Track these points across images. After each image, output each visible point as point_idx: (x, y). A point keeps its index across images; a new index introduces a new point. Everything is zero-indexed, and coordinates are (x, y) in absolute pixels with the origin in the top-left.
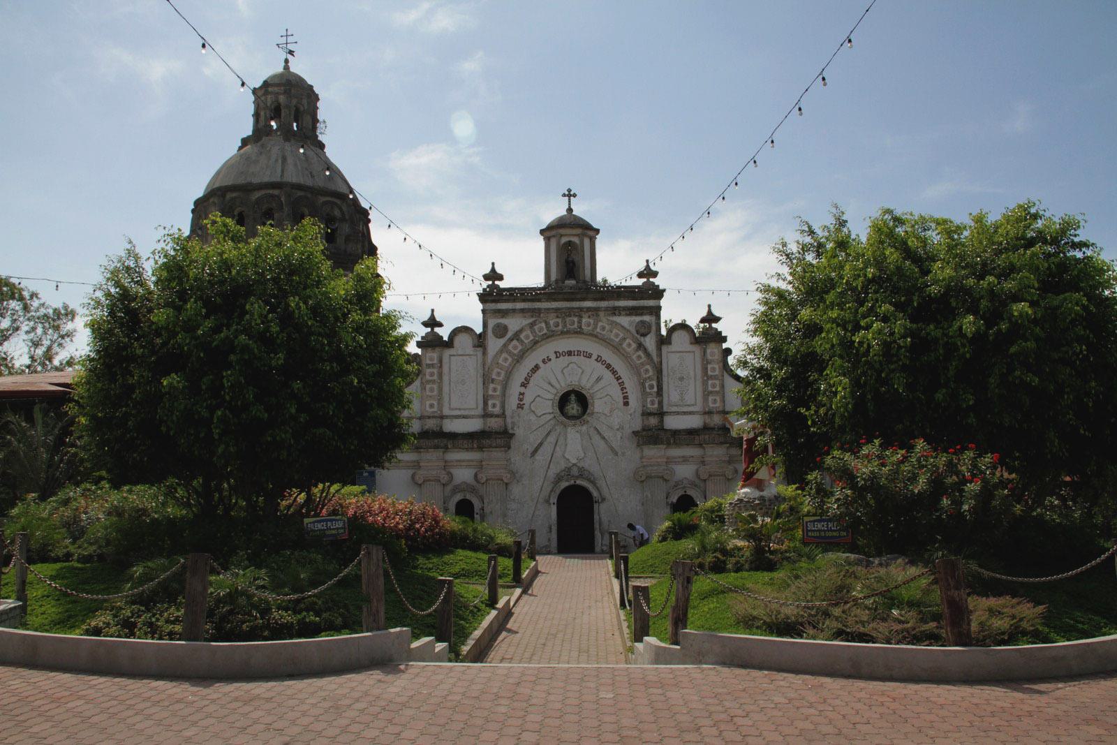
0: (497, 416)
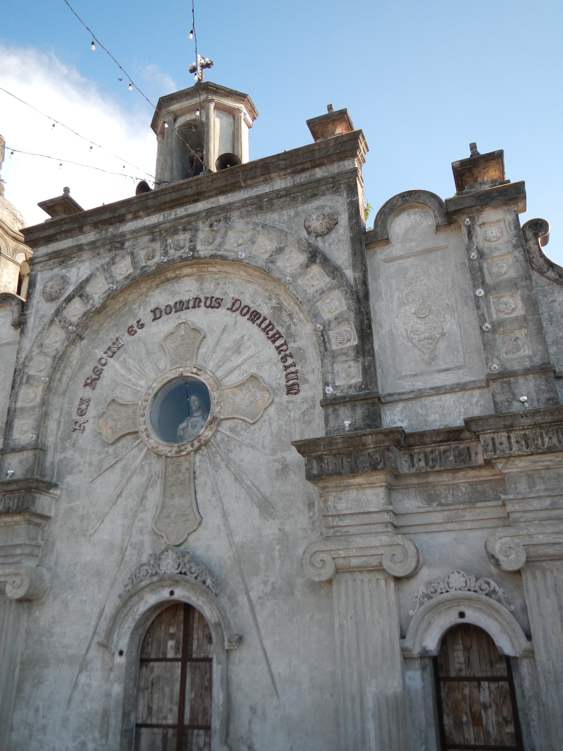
0: (22, 449)
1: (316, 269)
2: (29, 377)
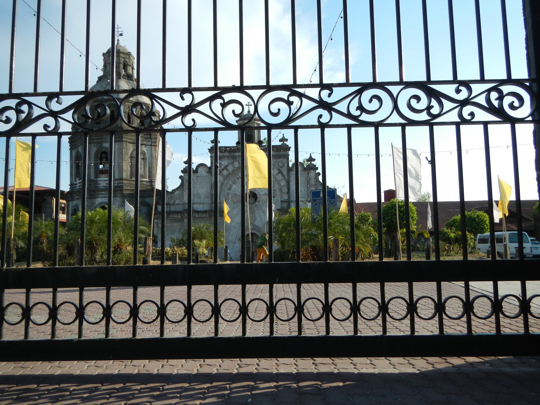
1: (280, 175)
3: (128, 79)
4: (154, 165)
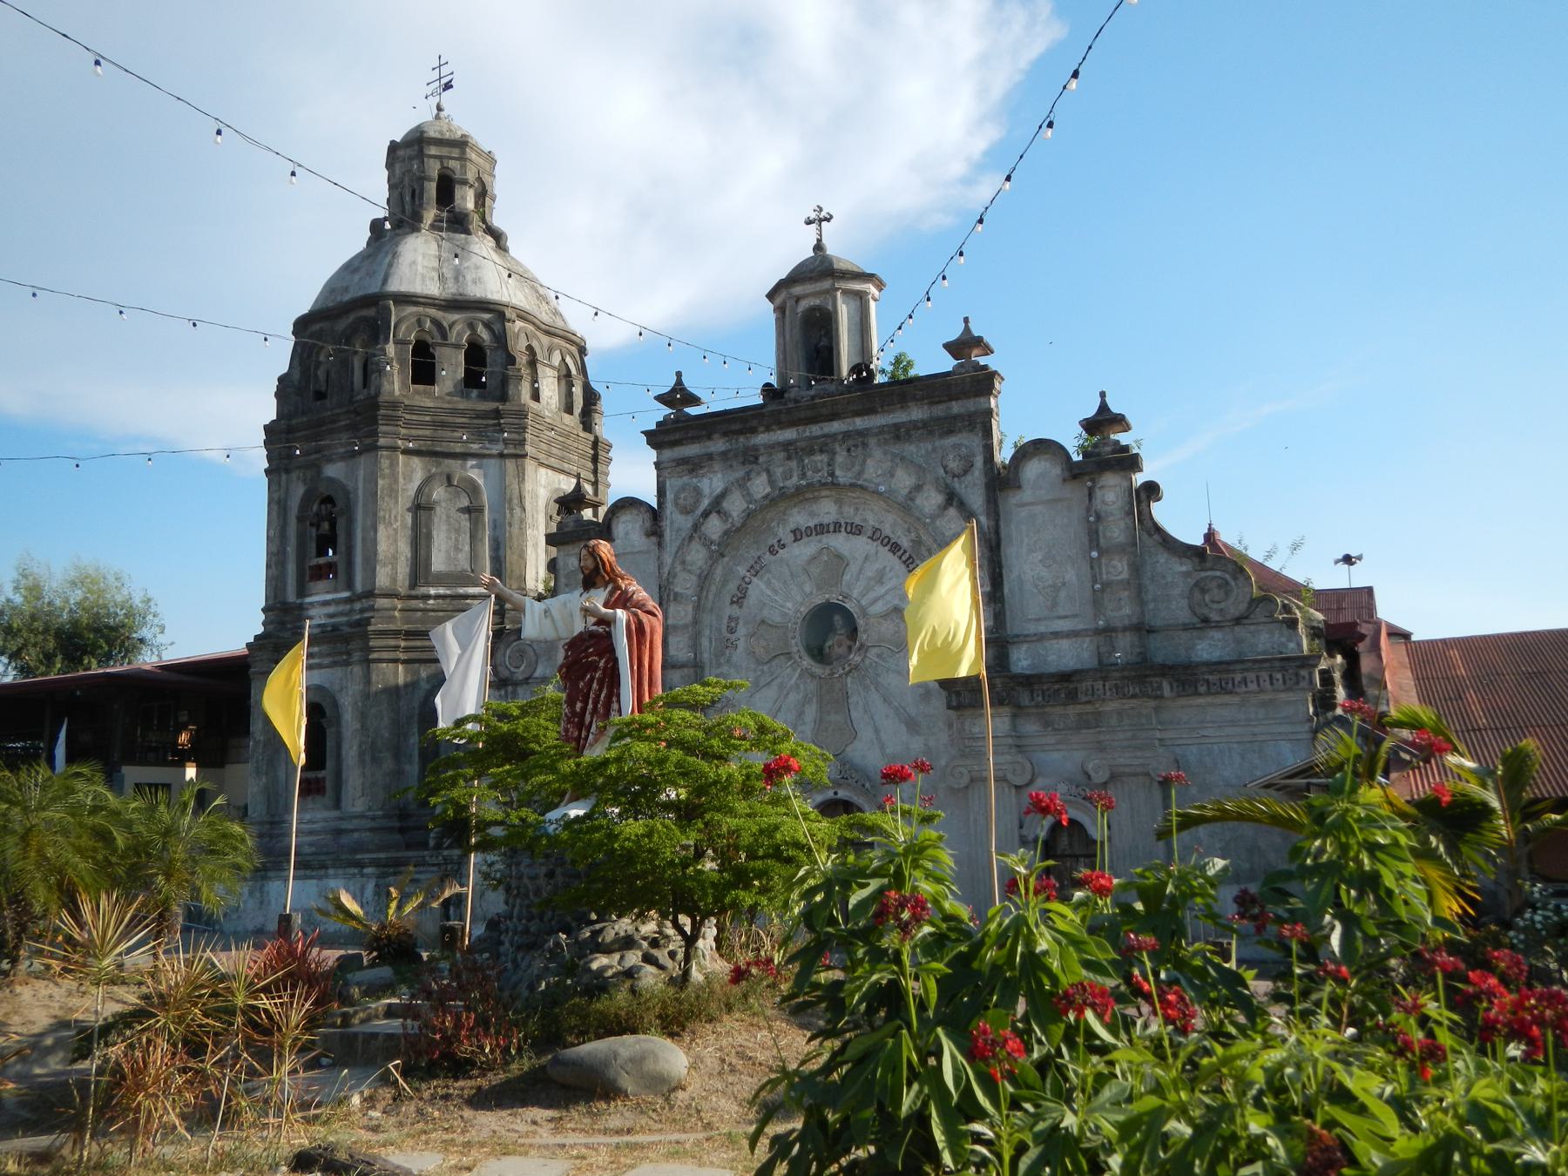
0: (682, 666)
1: (952, 512)
2: (676, 595)
3: (448, 229)
4: (515, 530)
